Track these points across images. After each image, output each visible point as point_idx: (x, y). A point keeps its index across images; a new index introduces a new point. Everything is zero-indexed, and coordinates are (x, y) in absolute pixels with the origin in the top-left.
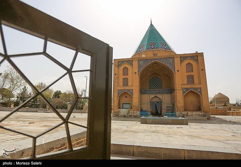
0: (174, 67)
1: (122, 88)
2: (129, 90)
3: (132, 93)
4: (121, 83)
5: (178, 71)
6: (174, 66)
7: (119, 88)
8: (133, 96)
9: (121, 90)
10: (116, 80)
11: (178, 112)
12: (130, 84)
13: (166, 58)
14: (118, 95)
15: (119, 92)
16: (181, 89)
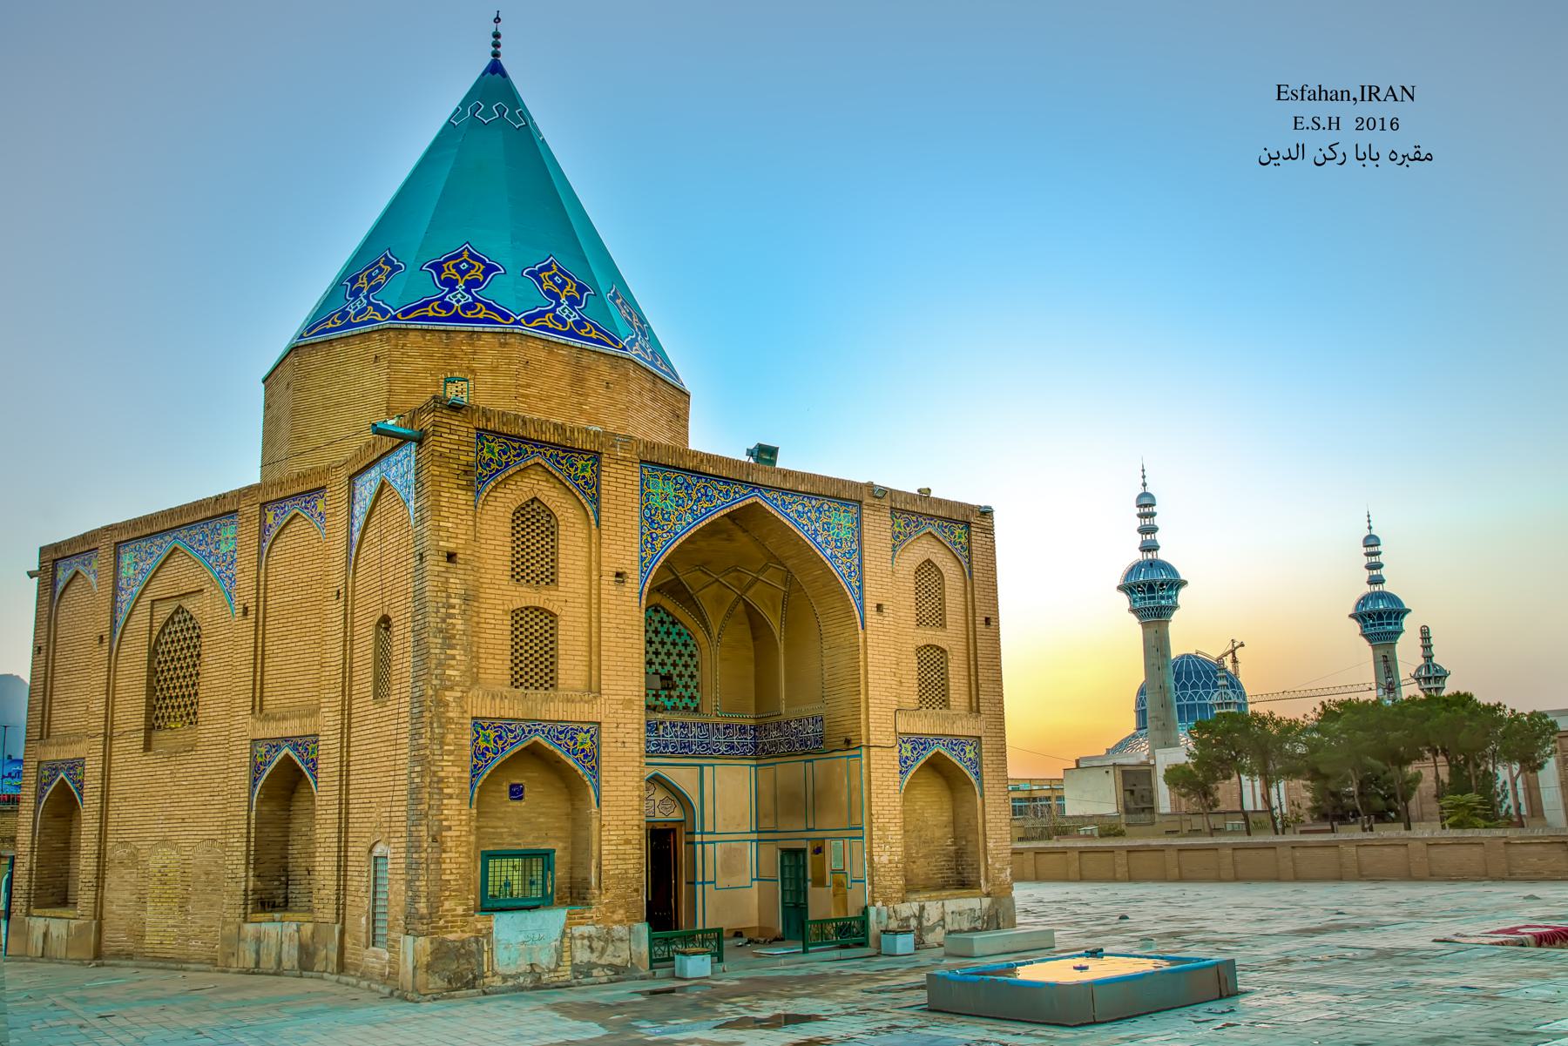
0: (861, 580)
1: (511, 707)
2: (567, 731)
3: (592, 758)
4: (497, 667)
5: (879, 607)
6: (861, 566)
7: (487, 709)
8: (598, 789)
9: (502, 727)
10: (459, 624)
11: (879, 904)
12: (571, 669)
13: (818, 495)
14: (475, 771)
15: (483, 744)
16: (891, 743)
